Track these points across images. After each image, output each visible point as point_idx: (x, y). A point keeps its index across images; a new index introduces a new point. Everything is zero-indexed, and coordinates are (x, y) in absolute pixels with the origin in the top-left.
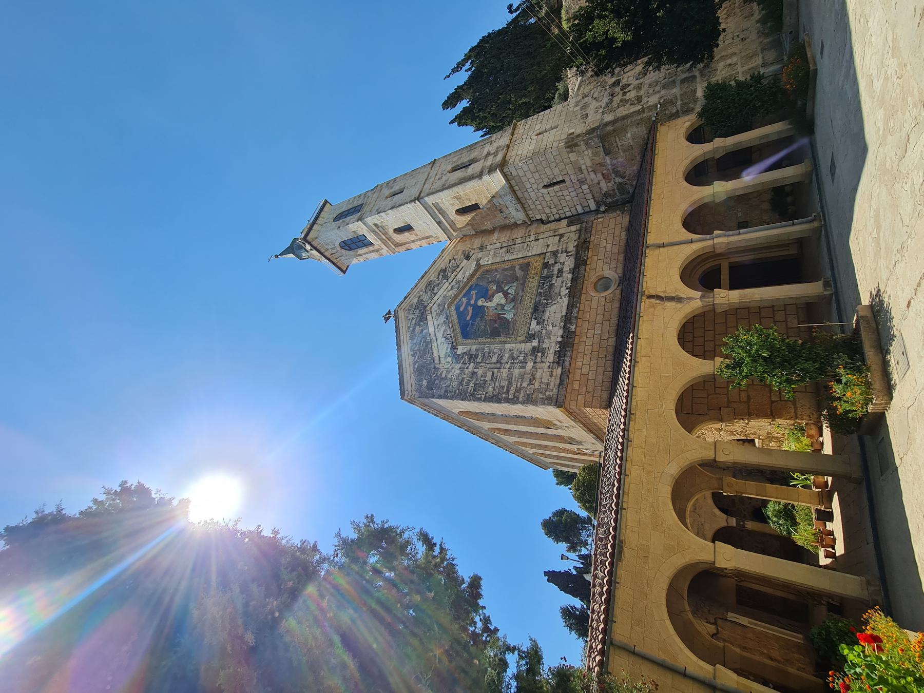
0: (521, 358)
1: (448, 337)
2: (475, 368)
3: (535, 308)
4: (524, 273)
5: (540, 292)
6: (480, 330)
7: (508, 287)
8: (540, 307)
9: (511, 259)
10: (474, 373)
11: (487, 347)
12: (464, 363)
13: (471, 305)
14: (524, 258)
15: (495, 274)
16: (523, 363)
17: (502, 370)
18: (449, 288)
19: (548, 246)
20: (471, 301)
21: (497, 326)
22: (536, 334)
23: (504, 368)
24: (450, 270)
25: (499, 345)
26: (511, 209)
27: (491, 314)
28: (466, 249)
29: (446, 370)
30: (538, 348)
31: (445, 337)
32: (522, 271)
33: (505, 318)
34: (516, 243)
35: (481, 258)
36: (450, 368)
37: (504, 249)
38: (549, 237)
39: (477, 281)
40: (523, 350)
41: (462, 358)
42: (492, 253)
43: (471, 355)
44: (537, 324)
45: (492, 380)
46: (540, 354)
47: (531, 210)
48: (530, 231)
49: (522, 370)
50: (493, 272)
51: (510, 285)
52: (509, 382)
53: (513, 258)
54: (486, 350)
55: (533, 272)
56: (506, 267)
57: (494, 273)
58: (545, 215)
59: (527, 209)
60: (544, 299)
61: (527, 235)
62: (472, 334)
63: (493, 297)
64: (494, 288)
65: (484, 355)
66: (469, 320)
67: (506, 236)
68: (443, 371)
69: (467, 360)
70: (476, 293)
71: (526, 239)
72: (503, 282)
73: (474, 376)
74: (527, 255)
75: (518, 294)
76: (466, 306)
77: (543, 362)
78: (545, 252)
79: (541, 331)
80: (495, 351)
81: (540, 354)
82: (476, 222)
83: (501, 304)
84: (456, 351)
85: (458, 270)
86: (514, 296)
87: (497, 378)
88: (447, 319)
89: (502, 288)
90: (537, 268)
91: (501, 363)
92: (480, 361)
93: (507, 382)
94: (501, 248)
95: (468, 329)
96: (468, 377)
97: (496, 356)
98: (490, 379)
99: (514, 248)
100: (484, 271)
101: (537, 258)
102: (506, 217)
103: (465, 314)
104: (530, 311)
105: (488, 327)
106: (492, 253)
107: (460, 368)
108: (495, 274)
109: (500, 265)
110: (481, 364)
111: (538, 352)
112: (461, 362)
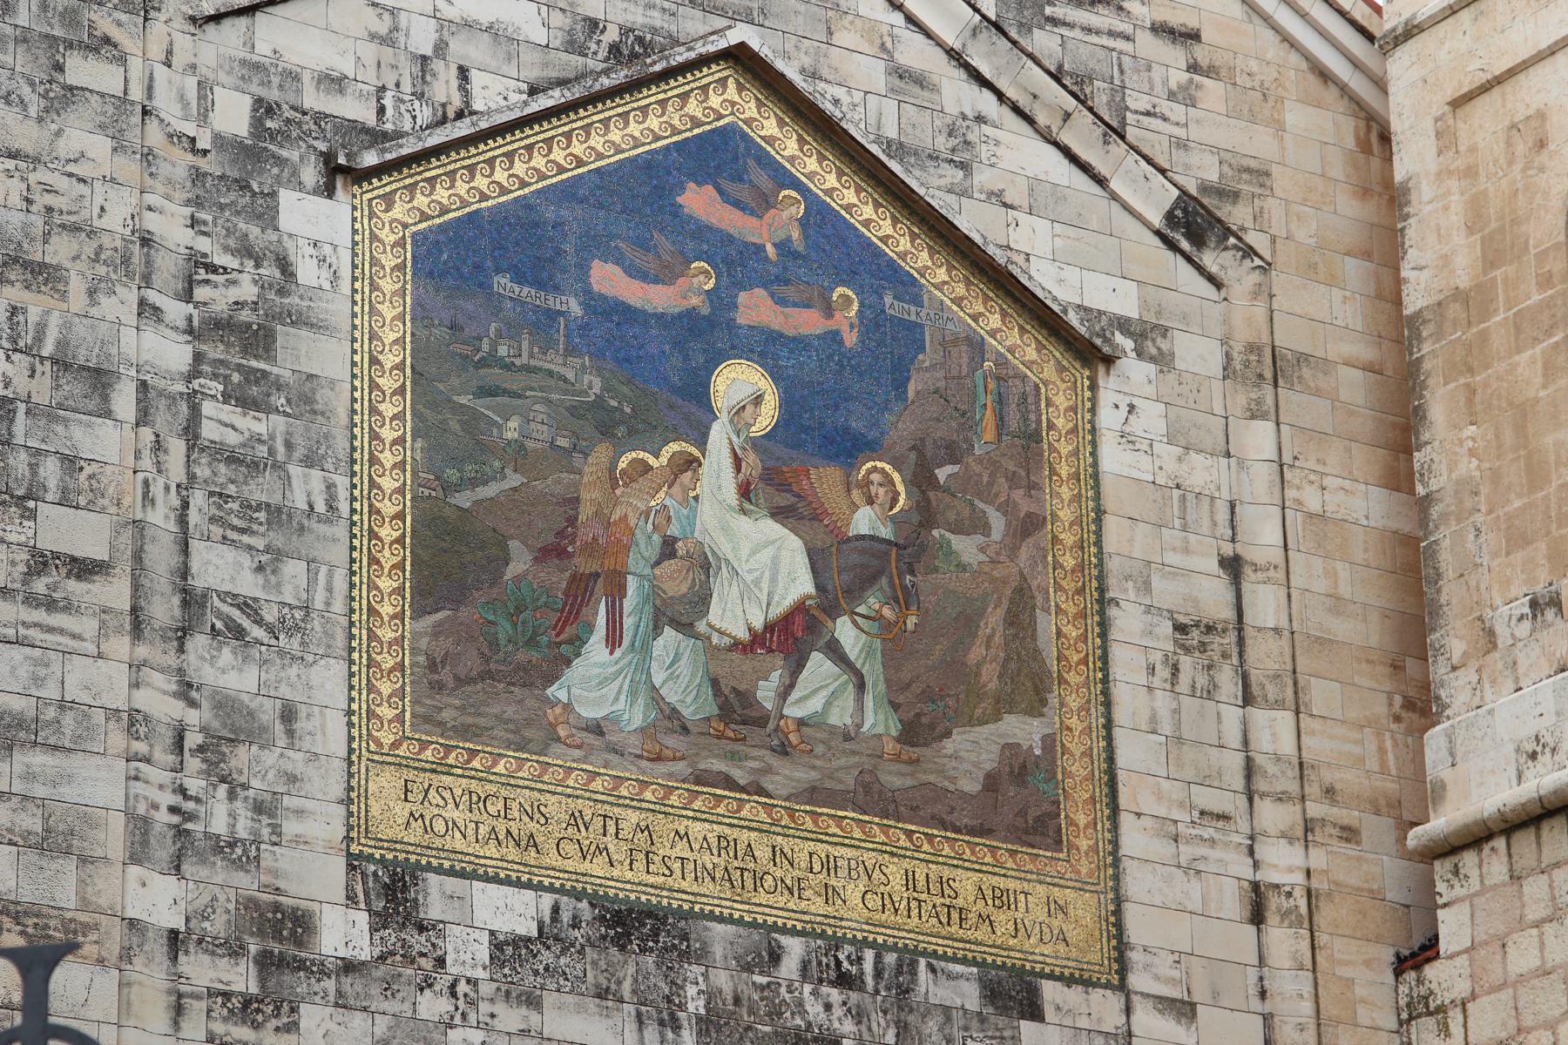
0: (219, 817)
1: (444, 88)
2: (143, 386)
3: (650, 912)
4: (963, 795)
5: (775, 957)
6: (483, 406)
7: (852, 657)
8: (650, 960)
9: (1117, 671)
10: (100, 379)
11: (330, 487)
12: (198, 267)
13: (722, 301)
14: (1101, 792)
15: (997, 522)
16: (180, 833)
17: (120, 646)
18: (915, 53)
19: (1184, 1010)
20: (760, 293)
21: (508, 575)
22: (418, 942)
23: (136, 666)
24: (1083, 53)
25: (339, 606)
26: (1549, 706)
27: (632, 504)
28: (1273, 206)
29: (137, 94)
30: (301, 965)
31: (441, 48)
32: (991, 782)
33: (578, 642)
34: (1258, 715)
35: (1163, 361)
36: (155, 136)
37: (1213, 598)
38: (1267, 1018)
39: (946, 344)
40: (290, 827)
41: (246, 251)
42: (1202, 472)
43: (258, 340)
44: (499, 945)
45: (41, 562)
46: (242, 978)
47: (1515, 878)
48: (1349, 834)
49: (113, 837)
50: (1018, 494)
51: (873, 672)
52: (20, 723)
53: (1120, 693)
54: (305, 487)
55: (966, 883)
56: (1046, 625)
57: (1006, 508)
58: (1462, 988)
59: (1523, 841)
60: (711, 995)
61: (1315, 810)
62: (453, 327)
63: (779, 514)
64: (864, 521)
65: (255, 467)
66: (592, 301)
67: (1336, 603)
68: (122, 60)
69: (217, 297)
70: (834, 337)
71: (1281, 798)
72: (904, 599)
73: (74, 388)
74: (1126, 820)
75: (784, 750)
76: (728, 239)
77: (178, 1010)
78: (1136, 981)
79: (443, 982)
80: (294, 569)
81: (242, 978)
82: (1497, 342)
83: (701, 600)
84: (311, 174)
85: (1083, 136)
86: (762, 721)
87: (51, 605)
88: (615, 49)
89: (854, 592)
90: (1000, 917)
91: (182, 634)
92: (209, 431)
93: (17, 704)
94: (1233, 566)
95: (503, 283)
96: (67, 326)
97: (249, 585)
98: (46, 544)
99: (1210, 693)
100: (1031, 399)
101: (1085, 910)
102: (1491, 633)
103: (644, 245)
104: (616, 873)
105: (514, 480)
106: (1202, 472)
107: (146, 241)
108: (997, 522)
109: (1069, 561)
110: (177, 447)
111: (266, 962)
112: (204, 244)
